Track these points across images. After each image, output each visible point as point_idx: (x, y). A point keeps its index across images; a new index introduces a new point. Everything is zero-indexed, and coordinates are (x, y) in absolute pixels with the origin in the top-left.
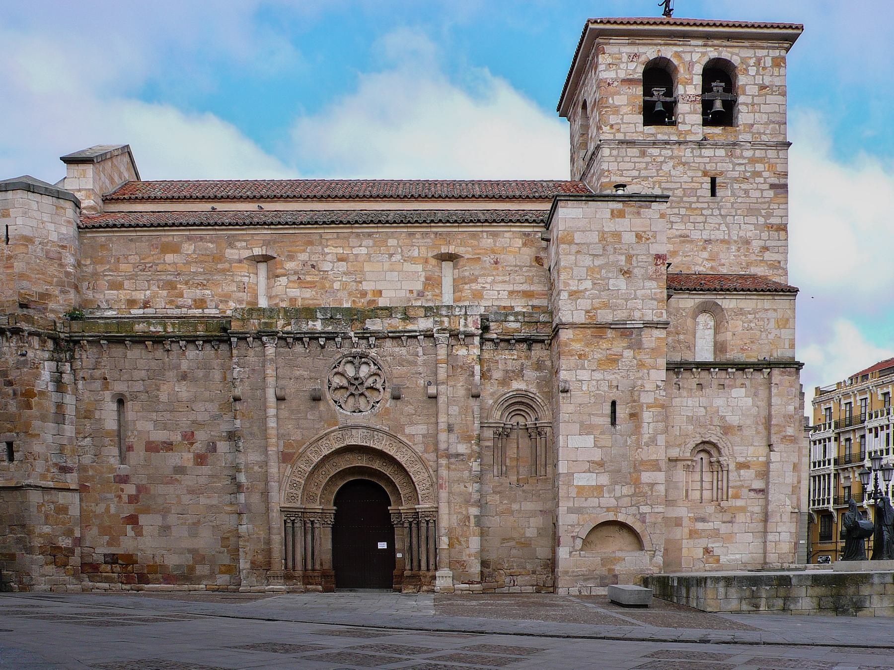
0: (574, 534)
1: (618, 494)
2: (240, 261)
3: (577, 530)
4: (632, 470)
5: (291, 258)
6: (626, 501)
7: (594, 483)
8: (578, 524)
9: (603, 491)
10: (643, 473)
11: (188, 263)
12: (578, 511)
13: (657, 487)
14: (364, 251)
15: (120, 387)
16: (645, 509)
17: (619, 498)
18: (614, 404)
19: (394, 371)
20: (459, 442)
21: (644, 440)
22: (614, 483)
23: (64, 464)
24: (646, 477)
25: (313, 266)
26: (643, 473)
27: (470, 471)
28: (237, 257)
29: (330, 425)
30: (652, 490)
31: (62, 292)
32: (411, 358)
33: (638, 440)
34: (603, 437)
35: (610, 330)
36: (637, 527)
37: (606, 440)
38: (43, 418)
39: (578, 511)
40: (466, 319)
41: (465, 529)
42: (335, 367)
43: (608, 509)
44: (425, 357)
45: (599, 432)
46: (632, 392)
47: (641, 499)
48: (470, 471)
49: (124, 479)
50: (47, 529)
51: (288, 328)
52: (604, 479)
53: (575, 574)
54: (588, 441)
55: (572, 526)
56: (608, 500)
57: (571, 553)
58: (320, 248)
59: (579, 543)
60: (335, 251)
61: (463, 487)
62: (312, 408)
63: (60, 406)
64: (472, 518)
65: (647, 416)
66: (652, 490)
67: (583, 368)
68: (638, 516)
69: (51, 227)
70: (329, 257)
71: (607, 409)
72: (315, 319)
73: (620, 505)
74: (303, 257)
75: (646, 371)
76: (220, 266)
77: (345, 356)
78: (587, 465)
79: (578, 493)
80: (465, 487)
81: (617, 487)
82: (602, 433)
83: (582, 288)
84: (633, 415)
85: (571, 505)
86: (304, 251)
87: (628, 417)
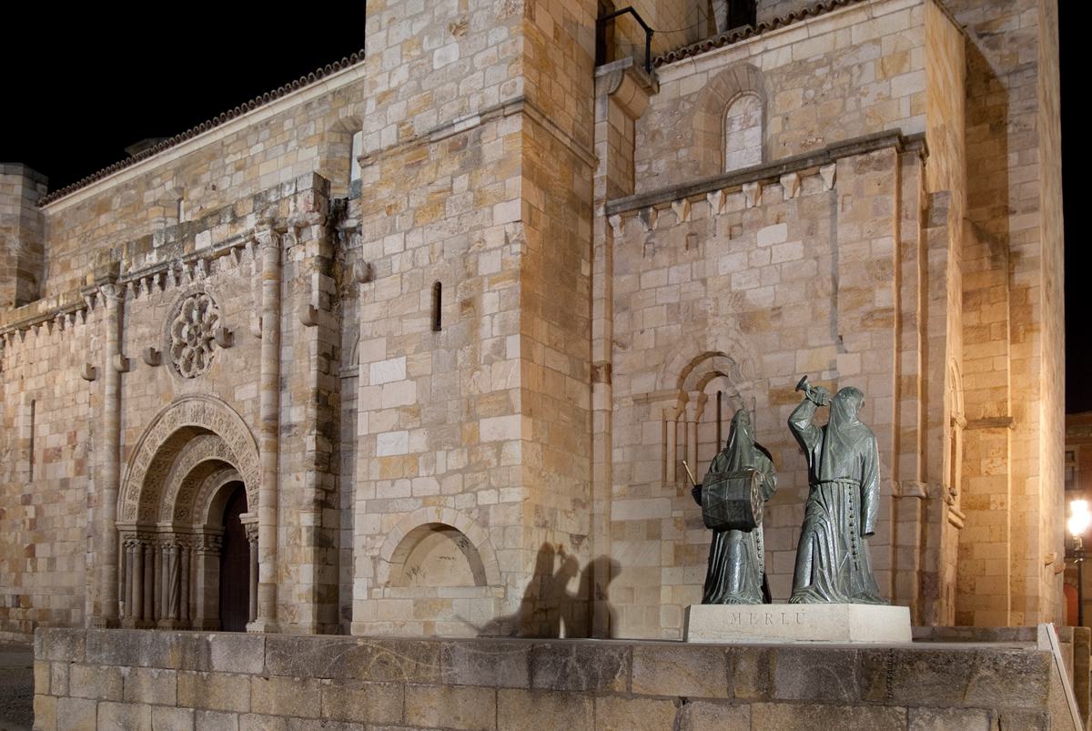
0: (376, 553)
1: (441, 470)
3: (379, 545)
4: (464, 418)
6: (454, 483)
7: (405, 451)
8: (380, 533)
9: (417, 464)
10: (482, 421)
12: (381, 506)
13: (507, 449)
16: (487, 497)
18: (438, 289)
19: (227, 306)
21: (485, 353)
22: (435, 446)
24: (489, 428)
27: (304, 452)
30: (498, 456)
32: (243, 281)
33: (474, 353)
35: (433, 146)
36: (473, 534)
37: (424, 363)
39: (381, 506)
41: (296, 550)
42: (177, 316)
43: (426, 500)
45: (414, 347)
47: (480, 476)
48: (304, 452)
49: (27, 500)
52: (419, 441)
54: (396, 368)
55: (372, 537)
56: (426, 484)
57: (370, 589)
61: (294, 480)
64: (304, 530)
66: (498, 456)
67: (393, 231)
71: (427, 302)
73: (444, 492)
75: (487, 210)
77: (183, 297)
78: (394, 418)
79: (383, 471)
80: (298, 479)
81: (441, 455)
82: (418, 351)
83: (394, 84)
84: (466, 304)
85: (371, 495)
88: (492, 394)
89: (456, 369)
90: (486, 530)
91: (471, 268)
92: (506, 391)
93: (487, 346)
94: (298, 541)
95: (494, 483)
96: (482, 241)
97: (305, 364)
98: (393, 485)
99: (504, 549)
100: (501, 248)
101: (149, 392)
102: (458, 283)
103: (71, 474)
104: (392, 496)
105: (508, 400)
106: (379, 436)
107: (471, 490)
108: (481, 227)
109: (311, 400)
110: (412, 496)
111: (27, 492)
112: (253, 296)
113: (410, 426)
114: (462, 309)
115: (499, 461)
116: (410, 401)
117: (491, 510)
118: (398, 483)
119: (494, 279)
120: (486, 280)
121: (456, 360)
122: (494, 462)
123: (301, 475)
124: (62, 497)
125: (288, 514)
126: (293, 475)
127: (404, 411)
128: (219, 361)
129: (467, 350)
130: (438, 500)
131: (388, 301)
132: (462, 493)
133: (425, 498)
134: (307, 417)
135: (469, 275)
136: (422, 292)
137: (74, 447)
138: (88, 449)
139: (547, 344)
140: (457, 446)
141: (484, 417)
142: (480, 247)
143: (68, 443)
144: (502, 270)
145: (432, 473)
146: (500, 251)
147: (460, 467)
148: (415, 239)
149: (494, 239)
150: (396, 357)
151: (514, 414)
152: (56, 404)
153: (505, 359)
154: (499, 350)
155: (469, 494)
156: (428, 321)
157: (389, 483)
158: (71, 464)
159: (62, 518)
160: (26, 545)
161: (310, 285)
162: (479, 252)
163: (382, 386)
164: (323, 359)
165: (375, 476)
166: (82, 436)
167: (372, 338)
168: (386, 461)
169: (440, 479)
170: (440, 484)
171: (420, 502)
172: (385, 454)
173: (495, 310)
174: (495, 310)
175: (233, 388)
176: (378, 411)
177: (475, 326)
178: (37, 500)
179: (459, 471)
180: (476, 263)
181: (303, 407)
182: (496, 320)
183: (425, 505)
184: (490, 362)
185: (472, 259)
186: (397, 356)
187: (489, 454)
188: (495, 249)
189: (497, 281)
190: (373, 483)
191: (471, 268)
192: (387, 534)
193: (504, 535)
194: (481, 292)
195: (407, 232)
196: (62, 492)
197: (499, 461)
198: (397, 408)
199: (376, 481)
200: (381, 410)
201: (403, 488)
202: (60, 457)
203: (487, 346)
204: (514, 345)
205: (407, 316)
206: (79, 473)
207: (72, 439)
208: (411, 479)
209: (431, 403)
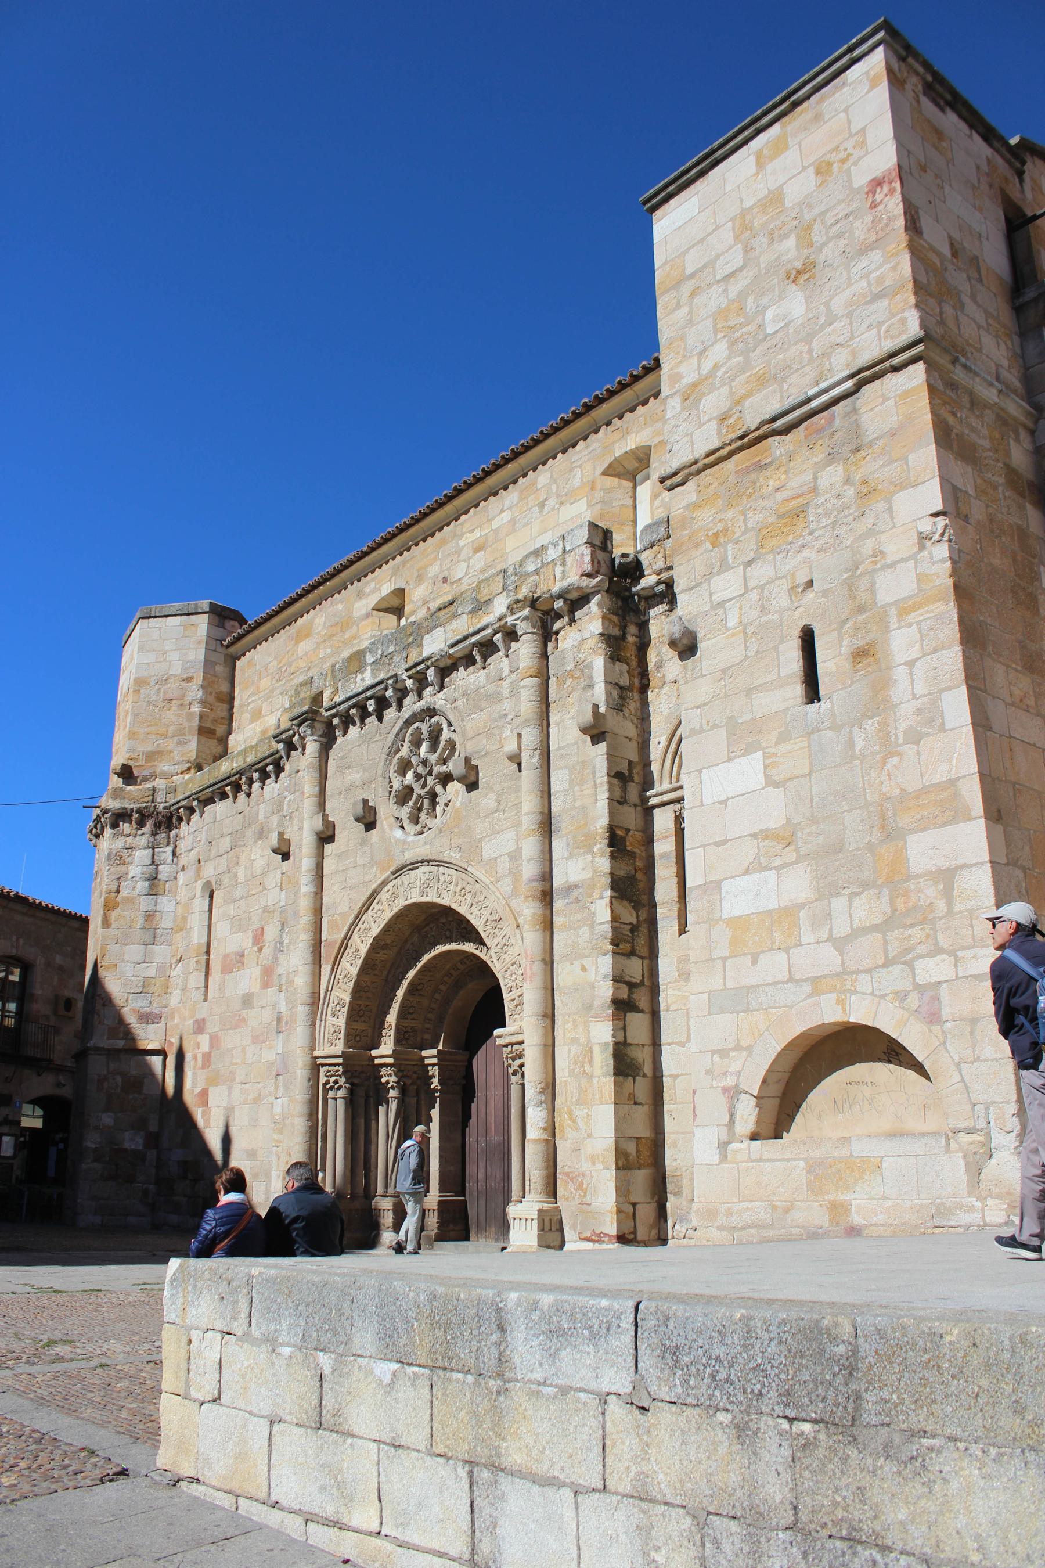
0: (730, 1081)
1: (842, 929)
2: (368, 616)
3: (735, 1067)
4: (876, 837)
5: (420, 579)
7: (772, 904)
8: (738, 1048)
10: (911, 839)
11: (318, 645)
12: (738, 1000)
14: (506, 516)
15: (209, 871)
17: (847, 939)
19: (468, 726)
20: (571, 856)
21: (903, 725)
22: (827, 890)
23: (148, 1010)
24: (924, 850)
25: (445, 580)
26: (911, 839)
28: (364, 612)
29: (383, 871)
30: (948, 894)
31: (179, 743)
32: (491, 688)
34: (784, 748)
38: (122, 941)
39: (738, 1000)
40: (563, 564)
41: (584, 1082)
43: (817, 985)
44: (513, 676)
45: (775, 734)
46: (850, 585)
47: (917, 933)
48: (592, 926)
50: (107, 1119)
51: (338, 699)
52: (797, 885)
53: (734, 1221)
54: (748, 772)
55: (723, 1053)
57: (723, 1146)
58: (453, 544)
59: (747, 1114)
60: (470, 537)
61: (578, 969)
62: (363, 843)
63: (149, 916)
64: (597, 1050)
65: (902, 642)
66: (948, 894)
67: (724, 566)
68: (913, 1001)
69: (174, 656)
70: (464, 554)
72: (360, 669)
73: (852, 966)
74: (433, 570)
76: (347, 635)
77: (408, 723)
80: (584, 969)
81: (839, 904)
82: (783, 738)
84: (861, 654)
85: (716, 983)
86: (435, 559)
87: (847, 665)
88: (926, 790)
89: (853, 757)
90: (936, 1028)
91: (863, 597)
92: (953, 782)
93: (906, 715)
94: (587, 1069)
95: (942, 943)
96: (878, 553)
97: (589, 791)
98: (754, 962)
99: (977, 1059)
100: (912, 557)
101: (360, 861)
102: (844, 622)
103: (256, 988)
104: (754, 981)
105: (956, 795)
106: (726, 885)
107: (905, 958)
108: (871, 533)
109: (601, 846)
110: (791, 979)
111: (199, 1016)
112: (507, 704)
113: (778, 861)
114: (855, 663)
115: (950, 904)
116: (775, 821)
117: (944, 991)
118: (764, 960)
119: (905, 608)
120: (893, 611)
121: (851, 745)
122: (941, 906)
123: (588, 962)
124: (244, 1020)
125: (569, 1026)
126: (577, 964)
127: (766, 838)
128: (458, 804)
129: (872, 725)
130: (840, 980)
131: (724, 671)
132: (884, 966)
133: (815, 981)
134: (595, 871)
135: (861, 609)
136: (781, 647)
137: (260, 950)
138: (279, 948)
139: (1009, 700)
140: (866, 886)
141: (913, 831)
142: (876, 563)
143: (254, 944)
144: (920, 590)
145: (825, 937)
146: (911, 564)
147: (877, 921)
148: (761, 572)
149: (897, 545)
150: (743, 755)
151: (970, 819)
152: (239, 891)
153: (942, 729)
154: (931, 716)
155: (900, 966)
156: (798, 690)
157: (748, 960)
158: (257, 972)
159: (244, 1050)
160: (198, 1090)
161: (591, 678)
162: (875, 571)
163: (724, 802)
164: (615, 781)
165: (722, 950)
166: (271, 933)
167: (701, 731)
168: (739, 925)
169: (840, 944)
170: (841, 954)
171: (807, 988)
172: (736, 913)
173: (915, 652)
174: (915, 652)
175: (481, 840)
176: (718, 844)
177: (881, 685)
178: (212, 1027)
179: (875, 928)
180: (872, 589)
181: (589, 857)
182: (920, 669)
183: (815, 992)
184: (915, 737)
185: (863, 584)
186: (747, 752)
187: (930, 893)
188: (904, 560)
189: (913, 609)
190: (719, 962)
191: (863, 597)
192: (749, 1048)
193: (972, 1033)
194: (887, 630)
195: (750, 563)
196: (244, 1013)
197: (950, 904)
198: (754, 836)
199: (724, 960)
200: (725, 842)
201: (773, 965)
202: (243, 964)
203: (906, 715)
204: (957, 706)
205: (758, 688)
206: (266, 985)
207: (258, 938)
208: (787, 950)
209: (814, 820)
